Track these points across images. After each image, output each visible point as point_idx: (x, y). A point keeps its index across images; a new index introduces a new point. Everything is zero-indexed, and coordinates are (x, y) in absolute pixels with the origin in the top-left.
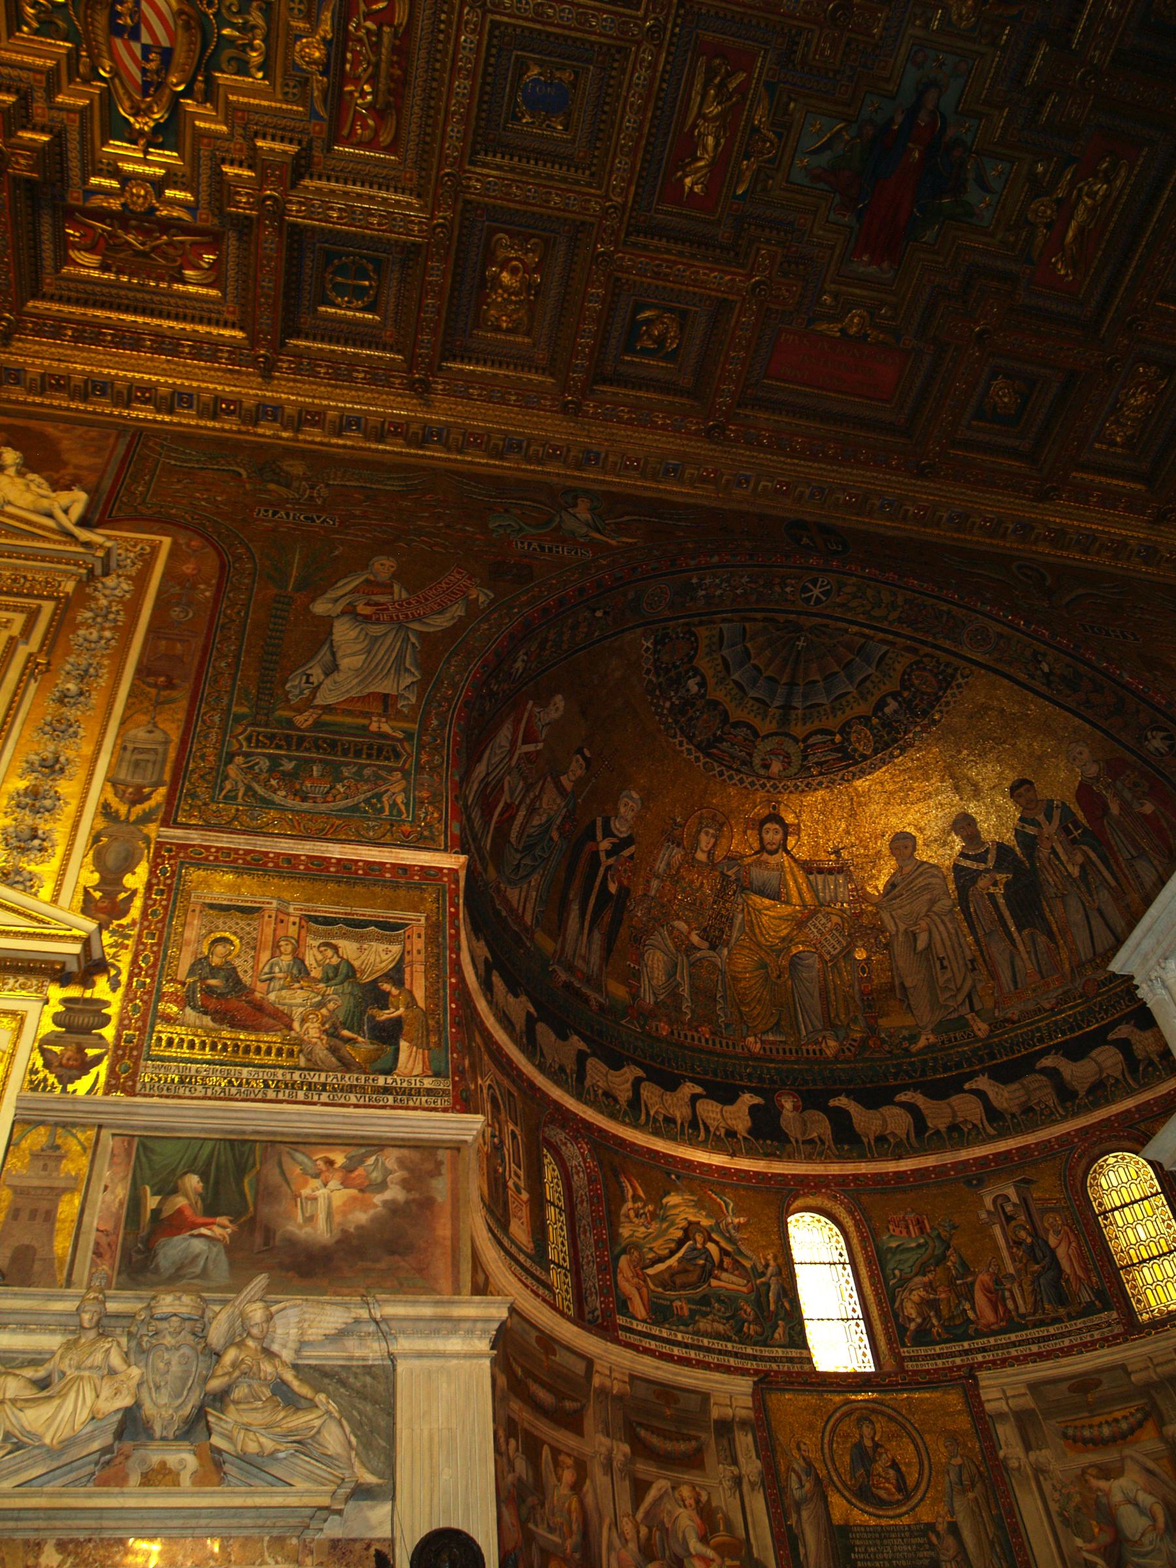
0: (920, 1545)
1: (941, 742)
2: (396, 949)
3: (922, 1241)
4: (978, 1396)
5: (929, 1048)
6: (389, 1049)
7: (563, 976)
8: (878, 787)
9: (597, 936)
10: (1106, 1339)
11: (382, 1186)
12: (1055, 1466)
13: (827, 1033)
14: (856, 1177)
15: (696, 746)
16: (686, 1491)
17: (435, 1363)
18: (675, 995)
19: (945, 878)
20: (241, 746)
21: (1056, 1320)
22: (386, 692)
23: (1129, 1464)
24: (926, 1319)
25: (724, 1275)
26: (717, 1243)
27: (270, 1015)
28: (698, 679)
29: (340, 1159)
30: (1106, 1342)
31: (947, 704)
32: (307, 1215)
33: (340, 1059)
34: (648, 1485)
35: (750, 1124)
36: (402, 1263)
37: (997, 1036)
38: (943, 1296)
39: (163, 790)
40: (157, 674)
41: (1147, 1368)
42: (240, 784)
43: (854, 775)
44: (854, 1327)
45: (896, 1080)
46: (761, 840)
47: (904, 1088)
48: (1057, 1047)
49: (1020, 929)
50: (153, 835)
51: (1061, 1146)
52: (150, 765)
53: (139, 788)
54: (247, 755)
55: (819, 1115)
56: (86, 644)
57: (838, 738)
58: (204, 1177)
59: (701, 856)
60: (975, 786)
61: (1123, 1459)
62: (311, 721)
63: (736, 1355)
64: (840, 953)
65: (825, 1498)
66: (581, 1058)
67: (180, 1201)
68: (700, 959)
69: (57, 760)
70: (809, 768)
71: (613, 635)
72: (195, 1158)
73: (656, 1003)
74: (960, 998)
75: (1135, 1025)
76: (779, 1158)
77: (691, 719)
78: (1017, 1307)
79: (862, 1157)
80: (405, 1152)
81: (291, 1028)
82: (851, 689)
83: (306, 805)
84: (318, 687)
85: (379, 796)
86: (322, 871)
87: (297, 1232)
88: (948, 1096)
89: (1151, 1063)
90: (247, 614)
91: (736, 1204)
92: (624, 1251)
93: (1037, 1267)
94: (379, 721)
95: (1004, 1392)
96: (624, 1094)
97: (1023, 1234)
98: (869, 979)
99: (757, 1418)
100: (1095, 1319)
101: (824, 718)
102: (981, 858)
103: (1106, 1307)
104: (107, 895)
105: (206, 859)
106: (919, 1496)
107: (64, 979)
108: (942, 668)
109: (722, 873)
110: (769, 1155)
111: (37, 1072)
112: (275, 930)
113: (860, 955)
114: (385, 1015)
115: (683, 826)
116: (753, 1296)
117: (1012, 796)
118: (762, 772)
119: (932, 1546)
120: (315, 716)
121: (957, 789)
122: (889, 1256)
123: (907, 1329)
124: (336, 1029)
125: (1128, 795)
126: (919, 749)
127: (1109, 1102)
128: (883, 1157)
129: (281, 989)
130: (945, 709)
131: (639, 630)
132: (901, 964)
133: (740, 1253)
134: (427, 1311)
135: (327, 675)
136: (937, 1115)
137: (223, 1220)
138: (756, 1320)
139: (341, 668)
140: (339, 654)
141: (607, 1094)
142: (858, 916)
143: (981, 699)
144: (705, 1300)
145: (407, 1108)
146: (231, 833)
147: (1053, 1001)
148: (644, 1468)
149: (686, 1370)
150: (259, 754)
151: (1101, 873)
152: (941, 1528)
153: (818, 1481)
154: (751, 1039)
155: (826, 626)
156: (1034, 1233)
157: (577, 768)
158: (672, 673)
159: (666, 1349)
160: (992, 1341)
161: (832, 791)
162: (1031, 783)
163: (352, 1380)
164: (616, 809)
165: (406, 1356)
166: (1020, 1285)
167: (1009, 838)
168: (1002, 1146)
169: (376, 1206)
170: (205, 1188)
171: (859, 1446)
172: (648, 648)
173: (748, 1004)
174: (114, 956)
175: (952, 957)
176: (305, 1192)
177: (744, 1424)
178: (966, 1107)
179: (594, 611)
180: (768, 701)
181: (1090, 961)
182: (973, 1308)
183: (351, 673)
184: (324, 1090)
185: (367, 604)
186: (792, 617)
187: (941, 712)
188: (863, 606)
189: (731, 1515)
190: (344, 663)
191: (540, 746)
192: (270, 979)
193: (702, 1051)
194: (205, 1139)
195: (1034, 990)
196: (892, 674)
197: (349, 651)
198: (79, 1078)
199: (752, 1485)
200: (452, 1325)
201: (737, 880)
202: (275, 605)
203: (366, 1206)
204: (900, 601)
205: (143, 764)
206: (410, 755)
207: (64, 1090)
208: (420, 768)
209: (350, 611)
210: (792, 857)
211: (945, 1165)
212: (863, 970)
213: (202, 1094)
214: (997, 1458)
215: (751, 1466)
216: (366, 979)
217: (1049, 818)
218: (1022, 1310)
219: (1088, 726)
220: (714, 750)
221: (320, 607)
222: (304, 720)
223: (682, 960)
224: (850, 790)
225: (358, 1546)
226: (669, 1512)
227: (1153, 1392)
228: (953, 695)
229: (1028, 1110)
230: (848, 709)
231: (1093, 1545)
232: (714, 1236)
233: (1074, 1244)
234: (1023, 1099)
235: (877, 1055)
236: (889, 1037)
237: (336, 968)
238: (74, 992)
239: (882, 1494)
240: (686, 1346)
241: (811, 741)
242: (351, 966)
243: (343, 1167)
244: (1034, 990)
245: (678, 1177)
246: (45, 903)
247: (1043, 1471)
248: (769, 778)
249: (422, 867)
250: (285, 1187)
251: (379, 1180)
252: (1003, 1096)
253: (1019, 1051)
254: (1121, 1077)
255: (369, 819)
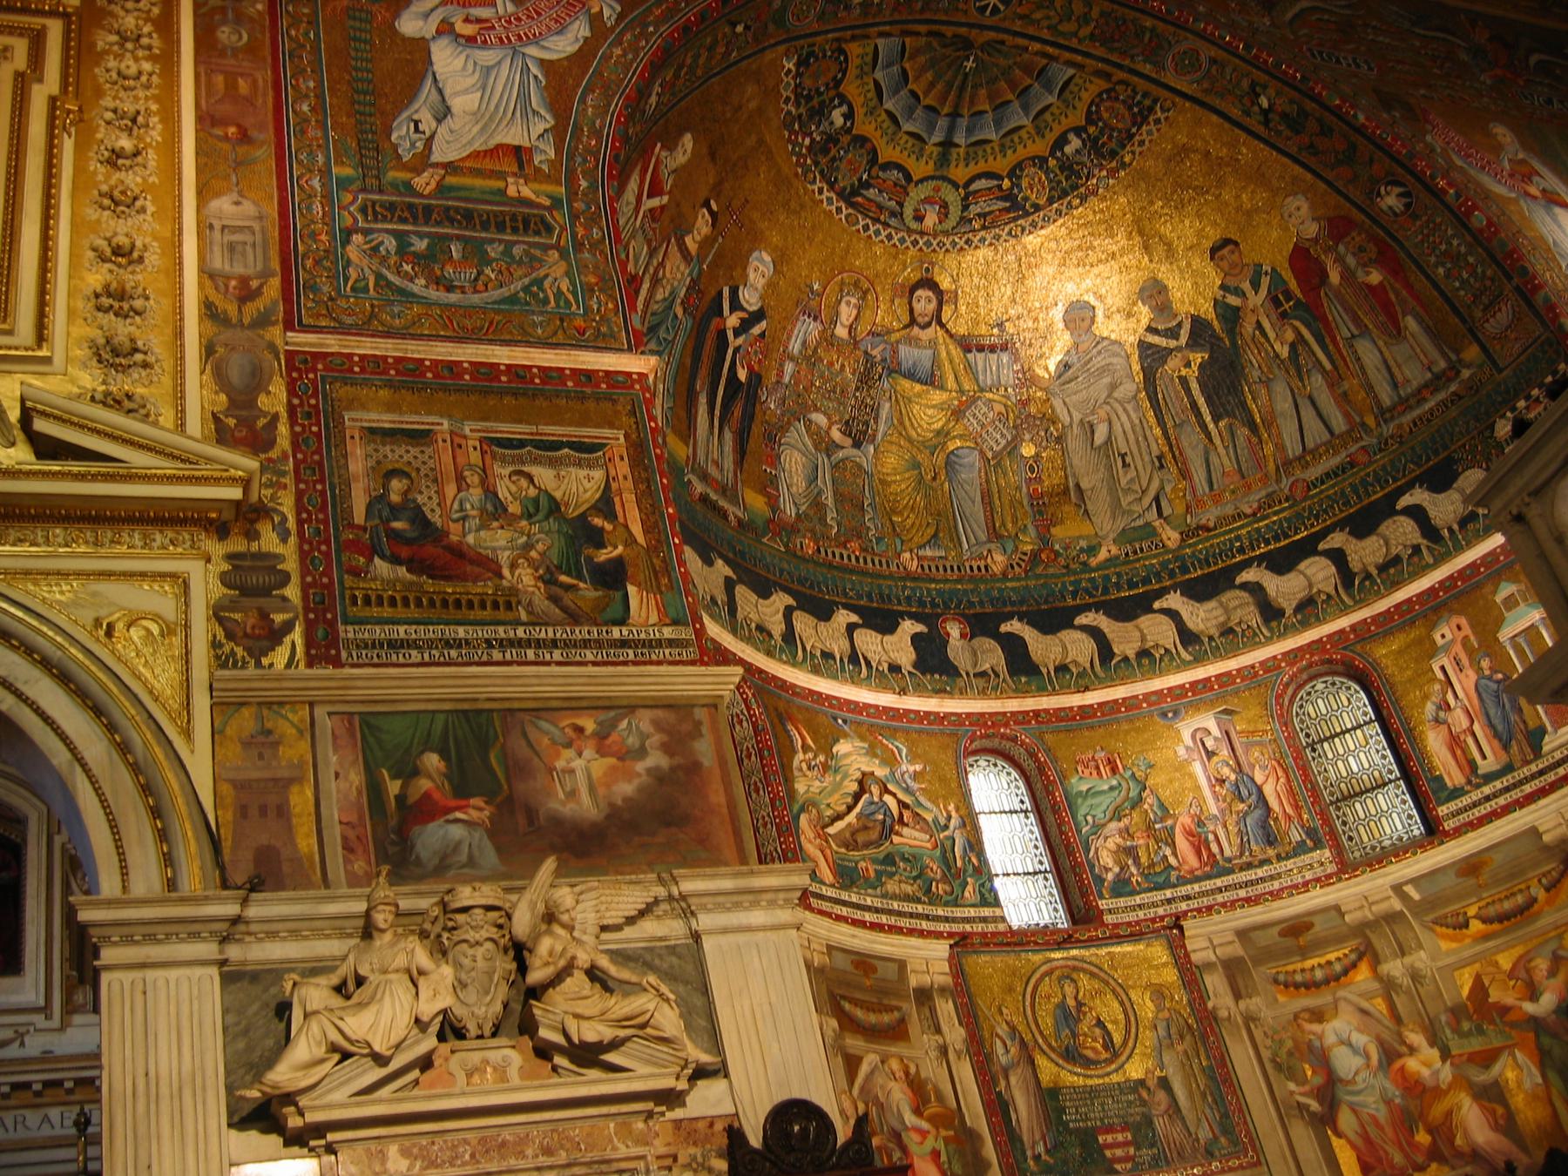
0: (1130, 1103)
1: (1130, 191)
2: (598, 474)
3: (1114, 782)
4: (1184, 946)
5: (1111, 561)
6: (618, 595)
7: (699, 488)
8: (1053, 245)
9: (728, 435)
10: (1318, 880)
11: (642, 752)
12: (1267, 1014)
13: (992, 546)
14: (1037, 713)
15: (838, 194)
16: (895, 1064)
17: (741, 938)
18: (818, 505)
19: (1128, 357)
20: (355, 220)
21: (1267, 861)
22: (516, 143)
23: (1342, 1005)
25: (905, 831)
26: (894, 795)
27: (472, 562)
28: (845, 108)
29: (589, 725)
30: (1323, 881)
31: (1142, 143)
32: (568, 789)
33: (564, 609)
34: (859, 1060)
35: (913, 656)
36: (681, 836)
37: (1190, 546)
38: (1141, 842)
39: (276, 282)
40: (224, 122)
41: (1362, 907)
42: (367, 270)
43: (1023, 230)
44: (1041, 882)
45: (1074, 599)
46: (911, 311)
47: (1085, 608)
48: (1260, 559)
49: (1216, 419)
50: (279, 342)
51: (1266, 672)
52: (249, 249)
53: (244, 281)
54: (366, 232)
55: (988, 643)
56: (121, 81)
57: (1006, 183)
58: (444, 754)
59: (841, 332)
60: (1170, 247)
61: (1336, 1002)
62: (433, 184)
63: (927, 917)
64: (1005, 448)
65: (1032, 1062)
66: (729, 585)
67: (424, 784)
68: (842, 460)
69: (133, 246)
70: (970, 221)
71: (755, 54)
72: (429, 734)
73: (797, 514)
74: (1147, 500)
75: (1350, 533)
76: (951, 694)
77: (834, 159)
79: (1042, 690)
80: (660, 713)
81: (501, 577)
82: (1025, 121)
83: (454, 297)
84: (432, 137)
85: (539, 282)
86: (491, 381)
87: (561, 808)
88: (1135, 617)
89: (1368, 576)
90: (317, 35)
91: (910, 750)
92: (802, 809)
94: (517, 184)
95: (1211, 941)
96: (777, 628)
97: (1226, 771)
98: (1039, 480)
99: (956, 984)
100: (1306, 859)
101: (991, 158)
102: (1173, 333)
103: (1318, 845)
104: (241, 421)
105: (351, 370)
106: (1127, 1052)
107: (222, 531)
108: (1139, 97)
109: (866, 353)
110: (939, 692)
111: (221, 645)
112: (454, 458)
113: (1028, 450)
114: (603, 555)
115: (821, 295)
116: (938, 852)
117: (1212, 258)
118: (914, 225)
119: (1144, 1103)
120: (437, 178)
121: (1146, 248)
123: (1103, 880)
124: (552, 574)
125: (1351, 261)
126: (1104, 199)
127: (1320, 621)
128: (1065, 689)
129: (478, 530)
130: (1138, 150)
131: (781, 48)
132: (1076, 461)
133: (920, 804)
134: (727, 884)
135: (439, 121)
136: (1125, 638)
137: (477, 801)
138: (944, 879)
139: (454, 110)
140: (447, 92)
141: (760, 628)
142: (1024, 404)
143: (1182, 139)
144: (889, 859)
145: (651, 663)
146: (373, 336)
147: (1255, 505)
148: (854, 1043)
149: (882, 937)
150: (380, 231)
151: (1314, 354)
152: (1152, 1083)
153: (1023, 1043)
154: (907, 555)
155: (1003, 42)
156: (1239, 769)
157: (703, 224)
158: (815, 101)
159: (858, 915)
160: (1196, 887)
161: (996, 249)
162: (1236, 244)
163: (657, 962)
164: (745, 277)
165: (710, 932)
167: (1207, 310)
168: (1200, 673)
169: (639, 775)
170: (449, 766)
171: (1062, 1005)
172: (789, 71)
173: (900, 513)
174: (273, 498)
175: (1135, 451)
176: (560, 764)
177: (943, 990)
178: (1157, 630)
179: (734, 25)
180: (925, 135)
181: (1299, 458)
182: (1175, 854)
183: (468, 118)
184: (556, 647)
185: (467, 20)
186: (963, 30)
187: (1133, 153)
188: (1048, 18)
189: (941, 1087)
190: (457, 104)
191: (665, 199)
192: (464, 519)
193: (852, 571)
194: (434, 712)
195: (1233, 492)
196: (1076, 102)
197: (458, 88)
198: (273, 649)
199: (958, 1054)
200: (753, 897)
201: (884, 360)
202: (351, 23)
203: (630, 775)
204: (1095, 13)
205: (239, 248)
206: (563, 229)
207: (259, 664)
208: (578, 246)
209: (446, 29)
210: (947, 331)
211: (1136, 697)
212: (1032, 469)
213: (419, 659)
214: (1206, 1009)
215: (955, 1034)
216: (572, 513)
217: (1256, 286)
218: (1227, 853)
219: (1309, 176)
220: (859, 199)
221: (409, 25)
222: (425, 182)
223: (822, 459)
224: (1018, 248)
225: (701, 1125)
226: (882, 1087)
227: (1368, 932)
228: (1149, 133)
229: (1227, 631)
230: (1020, 148)
231: (1307, 1088)
232: (890, 787)
234: (1222, 619)
235: (1051, 571)
236: (1066, 549)
237: (536, 501)
238: (237, 545)
239: (1089, 1053)
240: (877, 910)
241: (974, 187)
242: (552, 498)
243: (595, 734)
244: (1233, 492)
245: (845, 721)
246: (168, 430)
247: (1254, 1019)
248: (922, 233)
249: (607, 373)
250: (536, 759)
251: (637, 745)
252: (1200, 616)
253: (1216, 564)
254: (1333, 592)
255: (533, 313)
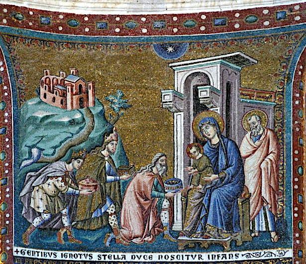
24: (56, 216)
78: (172, 222)
93: (214, 176)
97: (210, 131)
122: (30, 128)
156: (225, 131)
166: (185, 196)
233: (271, 156)
